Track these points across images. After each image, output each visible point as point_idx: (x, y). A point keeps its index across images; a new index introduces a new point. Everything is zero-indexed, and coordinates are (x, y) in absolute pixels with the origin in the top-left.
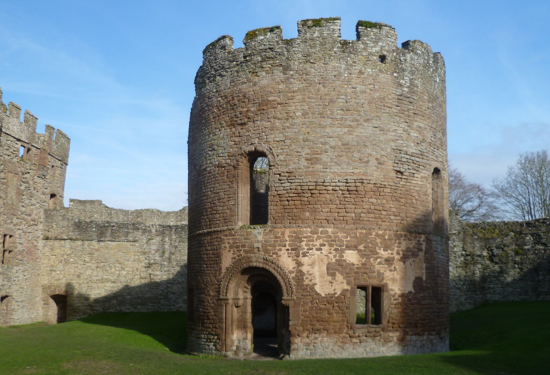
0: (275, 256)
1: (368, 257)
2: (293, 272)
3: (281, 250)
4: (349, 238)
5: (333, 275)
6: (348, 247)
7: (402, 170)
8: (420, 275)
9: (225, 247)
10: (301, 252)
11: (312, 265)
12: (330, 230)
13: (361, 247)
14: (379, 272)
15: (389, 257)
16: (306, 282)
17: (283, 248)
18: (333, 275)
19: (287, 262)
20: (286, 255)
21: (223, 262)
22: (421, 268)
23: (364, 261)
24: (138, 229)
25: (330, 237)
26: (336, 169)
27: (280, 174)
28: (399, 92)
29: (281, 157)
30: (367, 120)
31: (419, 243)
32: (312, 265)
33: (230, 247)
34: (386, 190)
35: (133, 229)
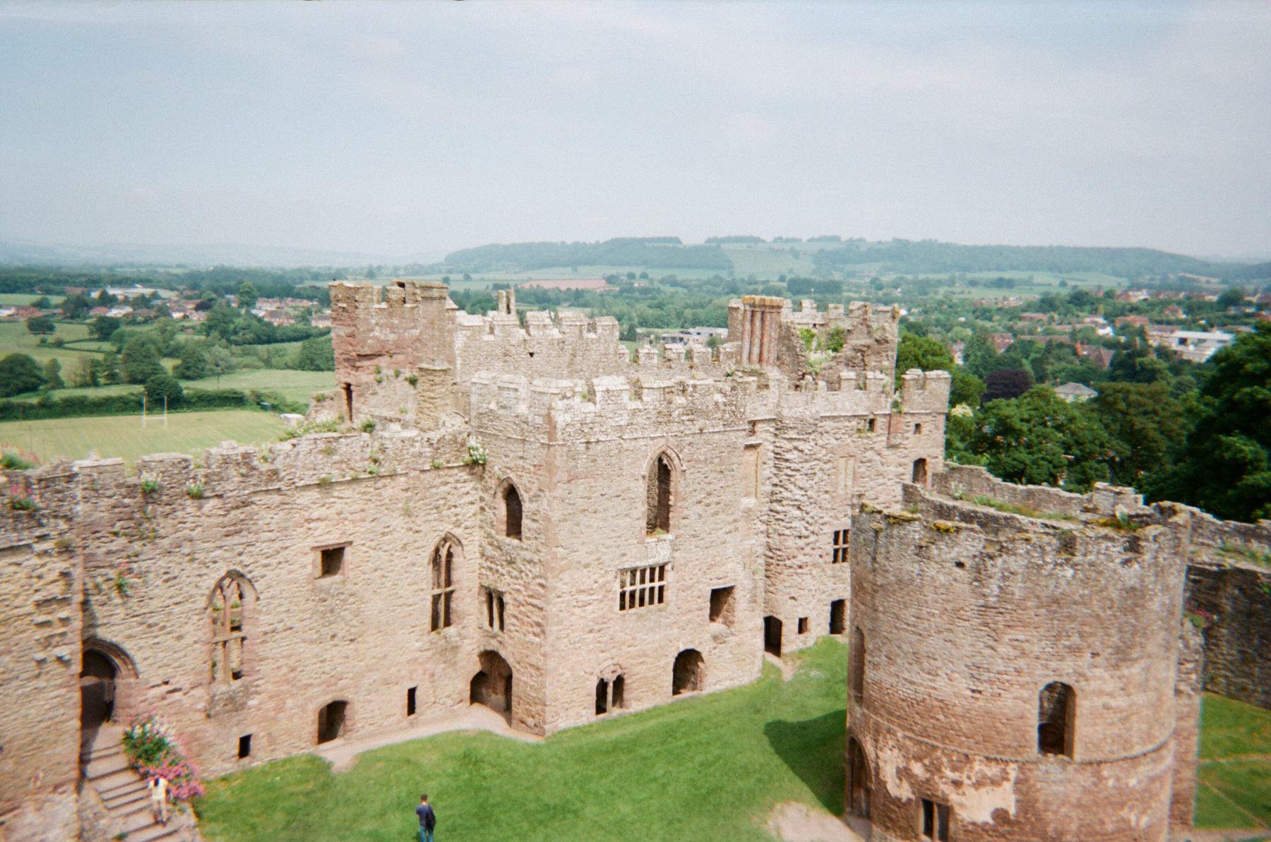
1: (933, 773)
13: (927, 762)
28: (981, 602)
30: (940, 632)
31: (1004, 771)
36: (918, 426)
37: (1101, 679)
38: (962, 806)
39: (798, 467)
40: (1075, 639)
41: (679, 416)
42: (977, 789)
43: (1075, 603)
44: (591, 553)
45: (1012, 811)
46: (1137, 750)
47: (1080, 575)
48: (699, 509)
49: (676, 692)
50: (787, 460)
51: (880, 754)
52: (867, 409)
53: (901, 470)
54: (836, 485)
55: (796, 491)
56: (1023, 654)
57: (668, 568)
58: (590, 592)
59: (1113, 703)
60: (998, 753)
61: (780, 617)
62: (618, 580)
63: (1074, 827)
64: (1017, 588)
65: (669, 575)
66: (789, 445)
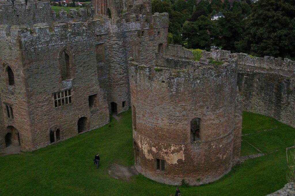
11: (144, 148)
12: (148, 139)
13: (157, 147)
14: (162, 156)
18: (149, 153)
30: (158, 105)
35: (188, 64)
36: (159, 32)
37: (210, 115)
38: (168, 159)
40: (201, 103)
41: (70, 36)
42: (173, 154)
43: (201, 91)
44: (42, 88)
46: (221, 136)
47: (202, 82)
48: (81, 69)
49: (79, 132)
50: (114, 48)
51: (143, 146)
52: (140, 28)
53: (154, 48)
56: (185, 110)
57: (72, 90)
58: (43, 102)
59: (214, 122)
60: (179, 142)
61: (116, 102)
62: (53, 97)
63: (203, 162)
65: (72, 93)
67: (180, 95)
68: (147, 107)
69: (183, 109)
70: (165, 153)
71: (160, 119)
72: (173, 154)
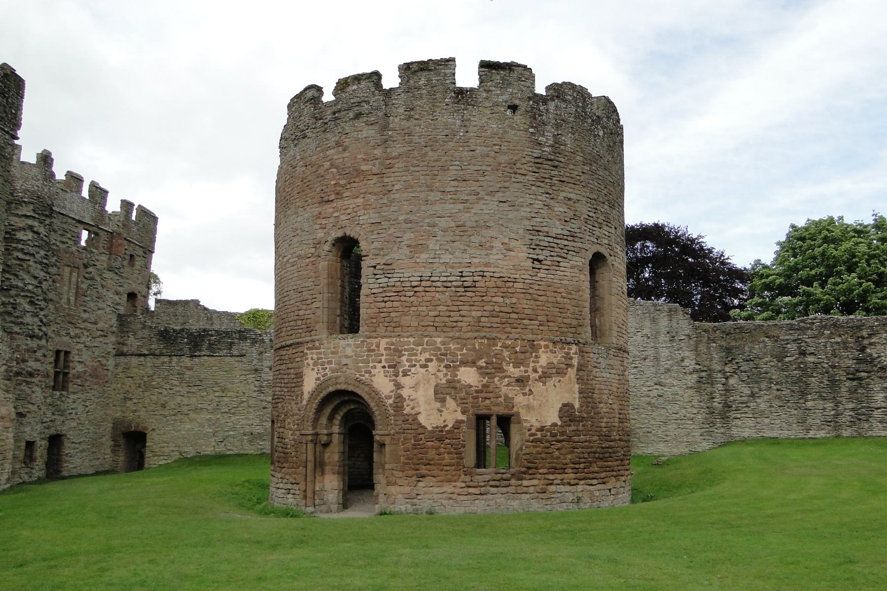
0: (367, 375)
1: (491, 376)
2: (390, 397)
3: (375, 367)
4: (465, 351)
5: (443, 401)
6: (464, 363)
7: (541, 257)
8: (570, 400)
9: (308, 364)
10: (401, 370)
11: (415, 387)
13: (482, 363)
14: (506, 397)
15: (521, 376)
16: (407, 410)
17: (379, 366)
18: (443, 401)
19: (382, 383)
20: (382, 374)
21: (305, 384)
22: (570, 391)
23: (485, 381)
24: (246, 339)
25: (440, 349)
26: (446, 258)
27: (375, 267)
28: (537, 153)
29: (376, 245)
31: (568, 357)
32: (415, 387)
33: (315, 364)
34: (516, 285)
35: (240, 339)
38: (529, 407)
39: (32, 250)
42: (544, 383)
45: (577, 406)
50: (19, 241)
51: (402, 380)
54: (60, 295)
55: (28, 279)
64: (568, 139)
66: (21, 223)
67: (562, 160)
68: (438, 207)
69: (572, 213)
70: (518, 381)
71: (497, 244)
72: (544, 383)
